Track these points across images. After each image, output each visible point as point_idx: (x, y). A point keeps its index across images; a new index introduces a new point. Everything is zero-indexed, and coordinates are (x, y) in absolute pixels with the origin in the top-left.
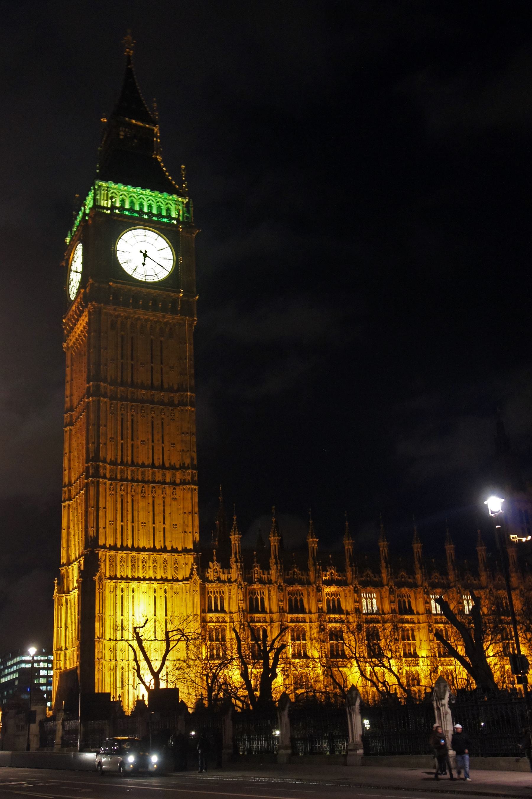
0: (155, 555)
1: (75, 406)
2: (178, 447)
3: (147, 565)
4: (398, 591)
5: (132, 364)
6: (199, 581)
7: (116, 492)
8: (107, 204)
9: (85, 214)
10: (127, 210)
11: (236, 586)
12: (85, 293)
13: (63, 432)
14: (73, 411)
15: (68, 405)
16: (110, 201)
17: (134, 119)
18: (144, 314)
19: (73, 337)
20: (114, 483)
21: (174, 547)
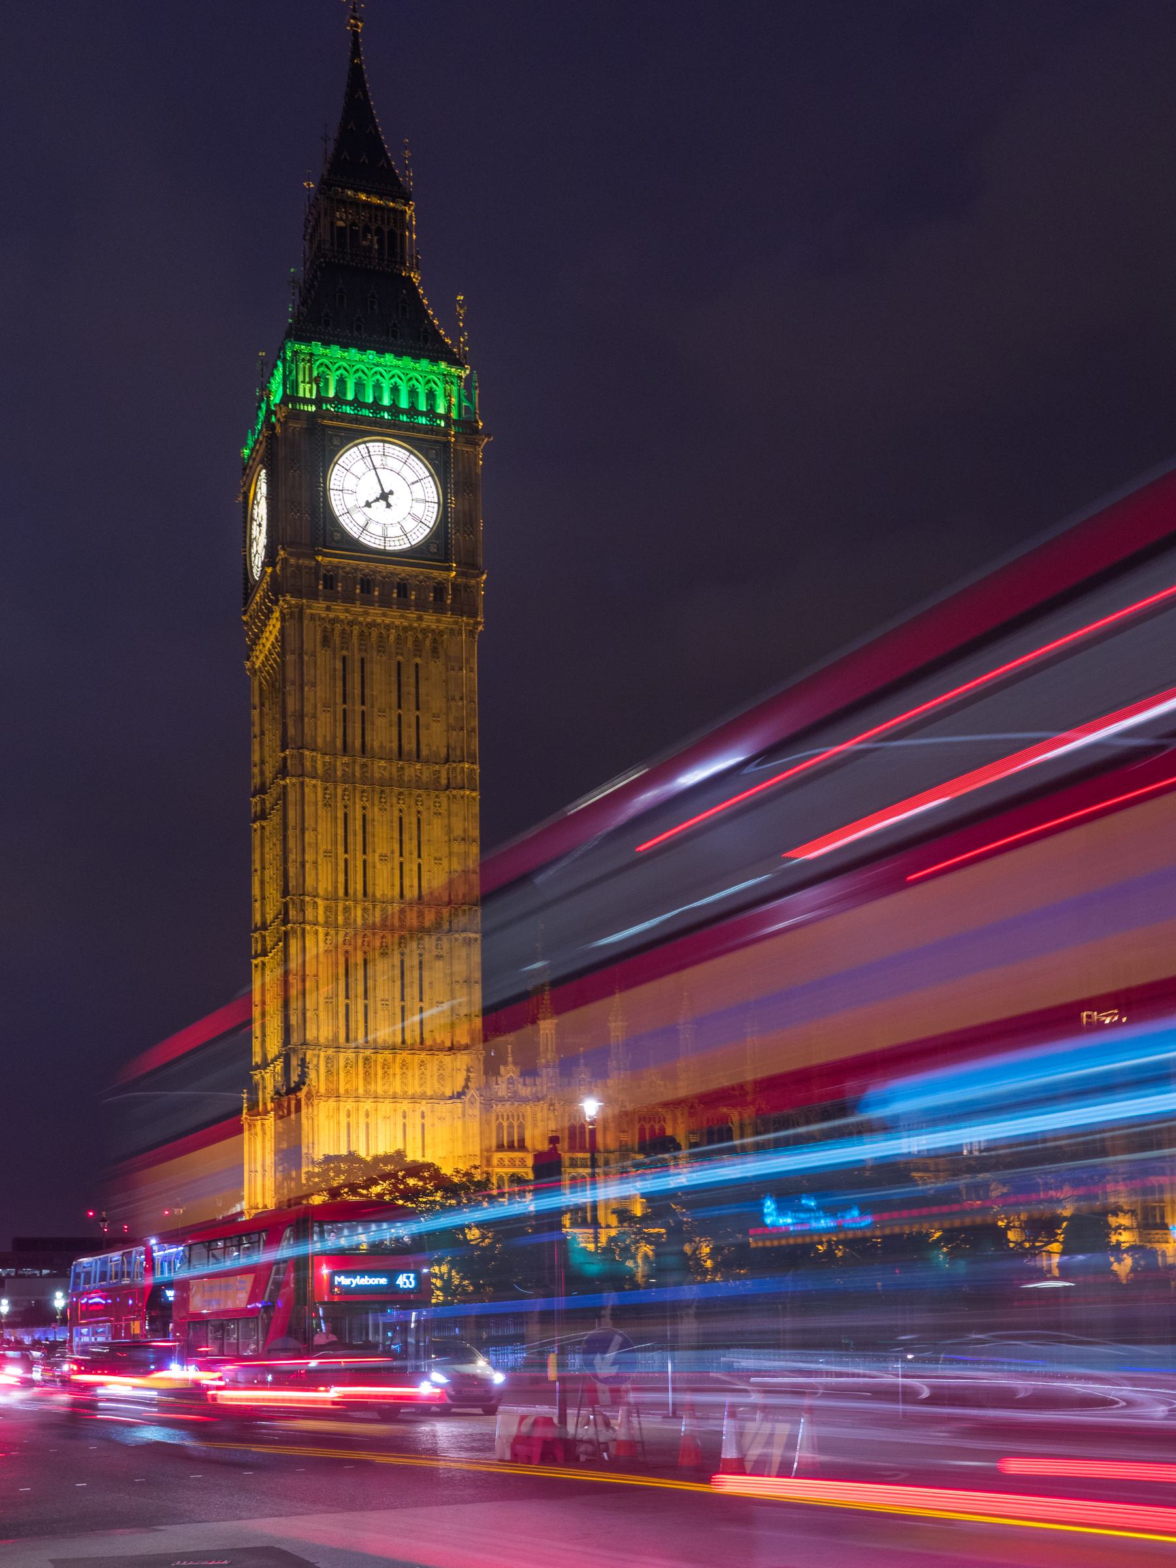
1: (268, 782)
3: (391, 1072)
5: (363, 713)
9: (270, 413)
11: (546, 1106)
12: (274, 572)
13: (249, 831)
14: (265, 793)
15: (257, 781)
17: (364, 191)
18: (384, 615)
21: (438, 1041)
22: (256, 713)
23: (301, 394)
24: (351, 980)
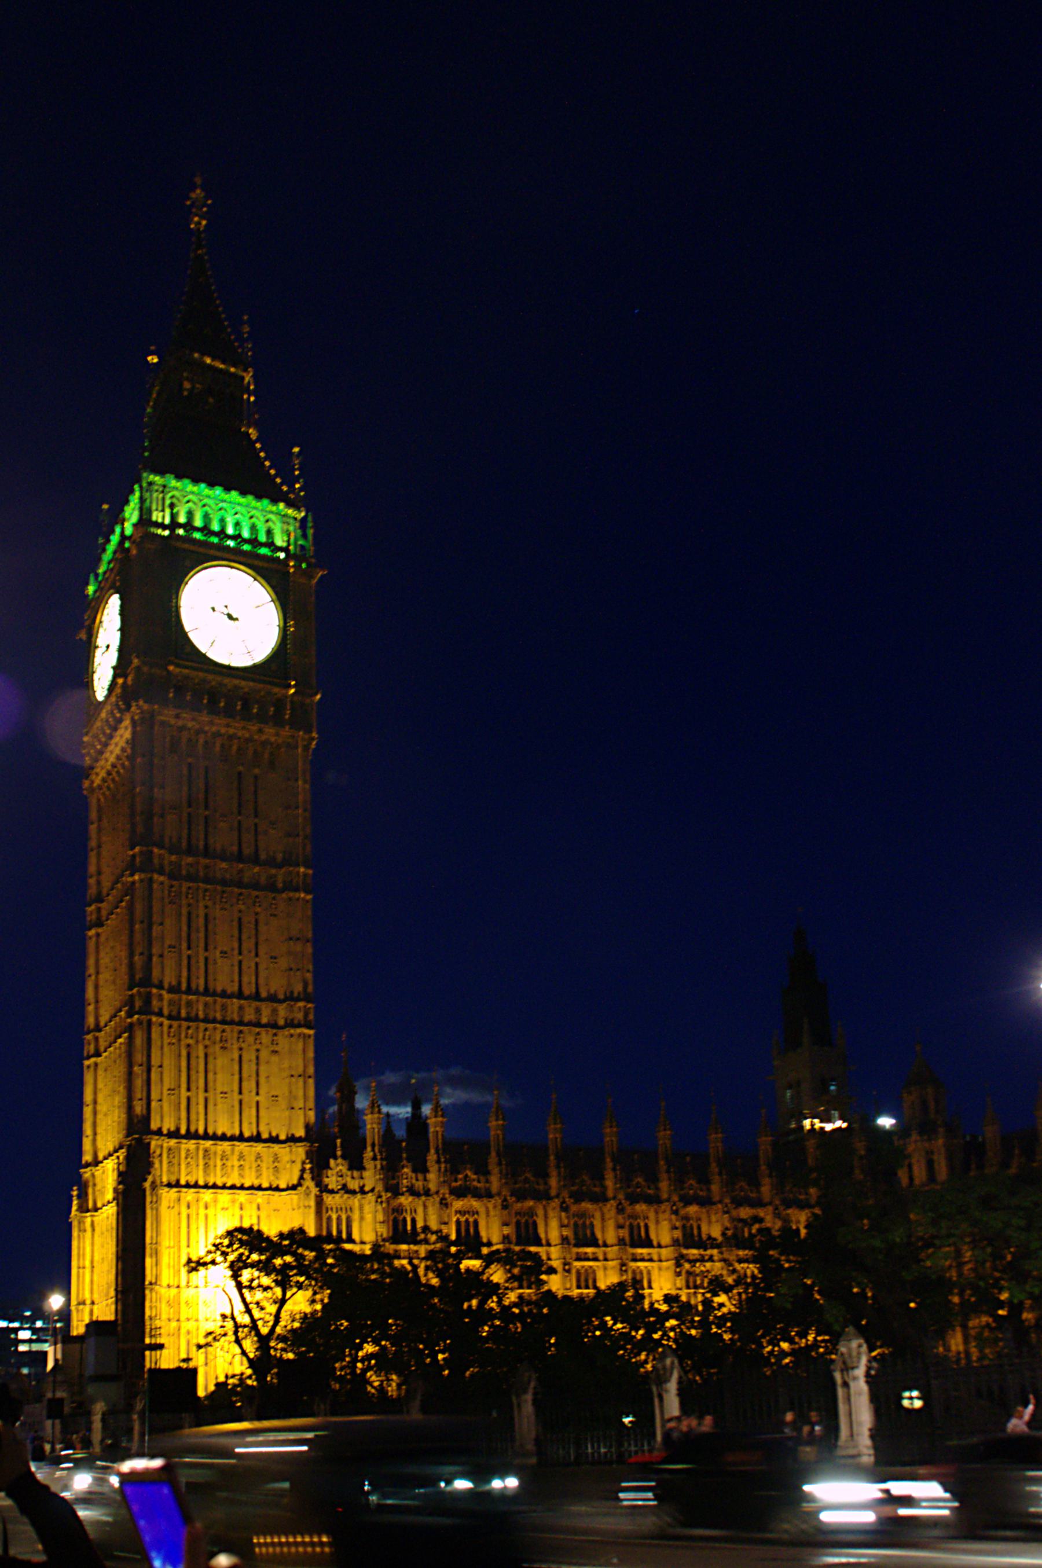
0: (242, 1146)
2: (283, 963)
3: (229, 1163)
4: (629, 1210)
6: (315, 1191)
7: (179, 1040)
8: (163, 517)
10: (197, 529)
16: (168, 511)
18: (228, 726)
19: (102, 768)
20: (175, 1024)
22: (93, 828)
23: (154, 518)
24: (193, 1073)
